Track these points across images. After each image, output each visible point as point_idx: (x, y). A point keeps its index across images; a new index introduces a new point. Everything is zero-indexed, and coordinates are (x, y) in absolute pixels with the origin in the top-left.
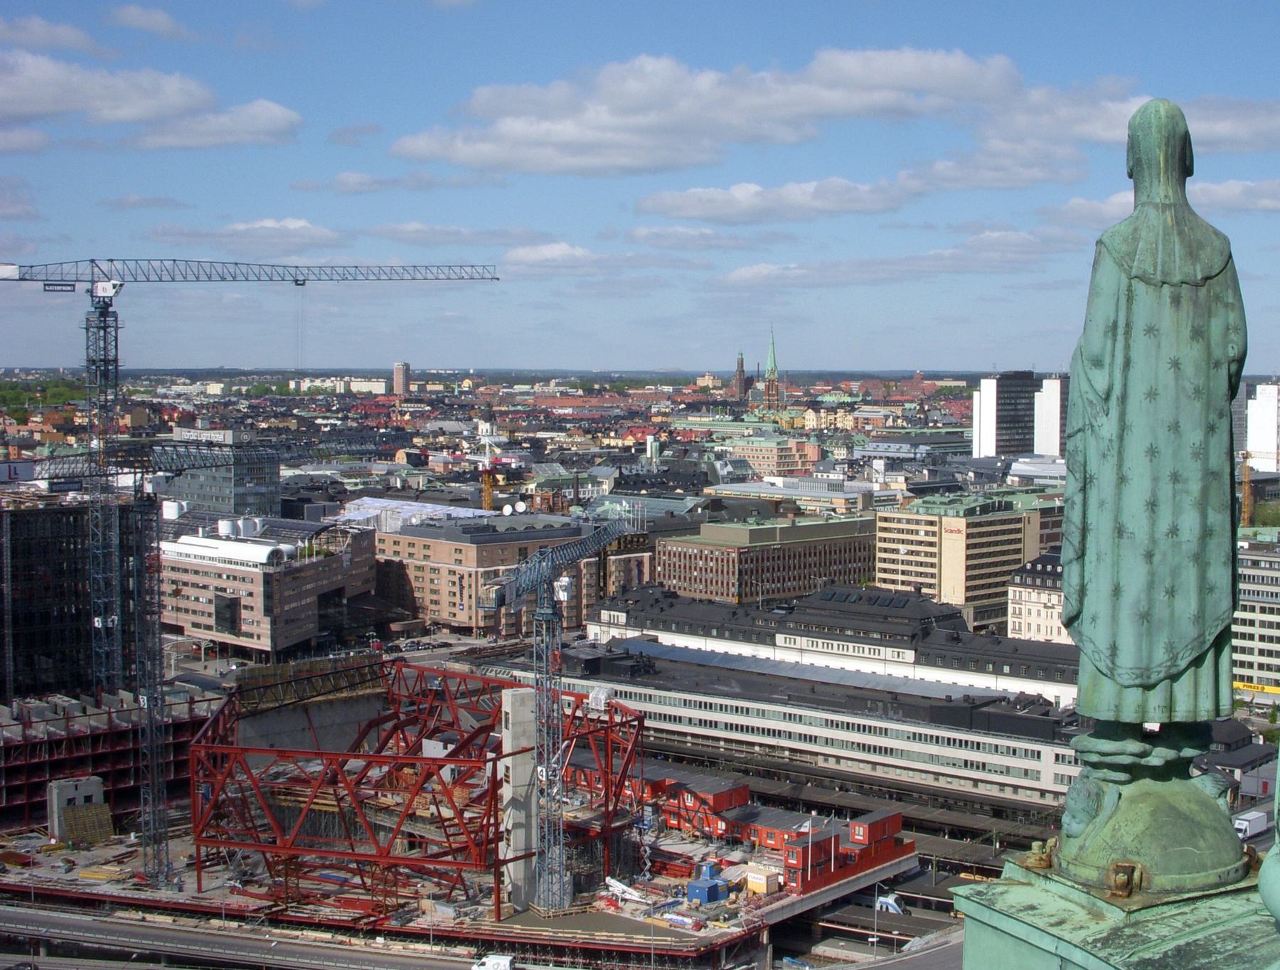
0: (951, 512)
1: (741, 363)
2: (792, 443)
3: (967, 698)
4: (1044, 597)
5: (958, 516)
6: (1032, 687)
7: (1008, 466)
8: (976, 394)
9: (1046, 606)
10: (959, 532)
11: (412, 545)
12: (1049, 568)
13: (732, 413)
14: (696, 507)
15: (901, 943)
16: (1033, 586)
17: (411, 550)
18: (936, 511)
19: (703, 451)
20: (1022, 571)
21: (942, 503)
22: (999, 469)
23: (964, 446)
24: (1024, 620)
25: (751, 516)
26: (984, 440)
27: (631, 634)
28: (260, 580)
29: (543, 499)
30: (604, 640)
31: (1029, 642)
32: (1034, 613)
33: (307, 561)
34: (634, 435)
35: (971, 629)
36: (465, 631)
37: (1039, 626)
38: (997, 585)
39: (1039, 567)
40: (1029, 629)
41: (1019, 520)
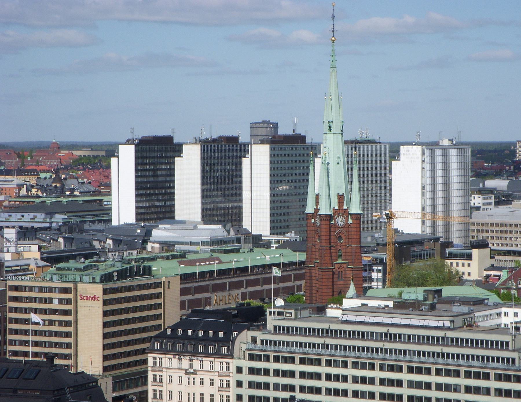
0: (86, 279)
4: (186, 363)
5: (94, 282)
7: (148, 233)
8: (114, 160)
9: (187, 372)
10: (95, 298)
12: (190, 332)
16: (174, 352)
20: (162, 336)
22: (138, 236)
24: (166, 387)
32: (175, 379)
37: (180, 393)
38: (136, 353)
39: (180, 332)
41: (158, 285)
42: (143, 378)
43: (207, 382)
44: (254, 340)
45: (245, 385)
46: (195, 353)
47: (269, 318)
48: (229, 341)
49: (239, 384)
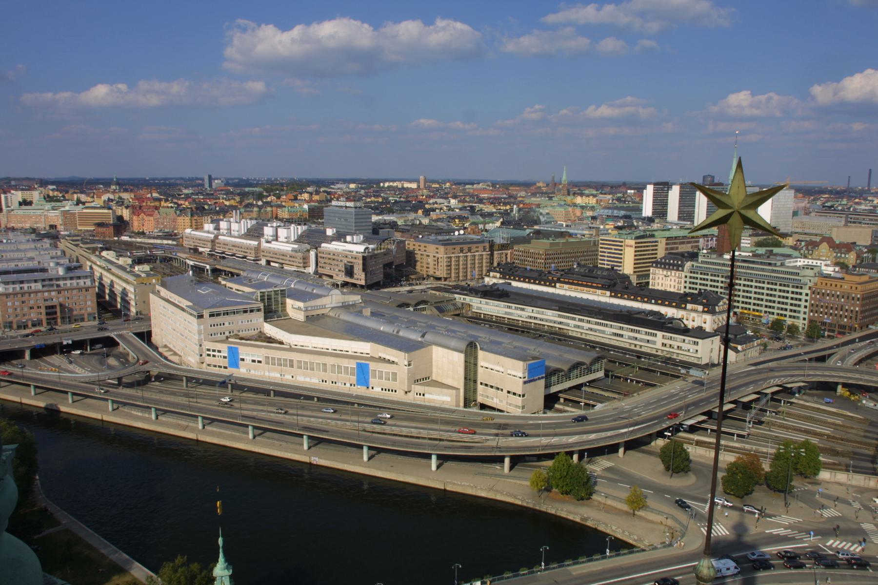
1: (553, 178)
2: (570, 209)
3: (628, 311)
4: (665, 273)
5: (632, 239)
6: (656, 308)
8: (645, 191)
9: (665, 276)
10: (631, 246)
11: (420, 246)
13: (548, 197)
14: (530, 233)
15: (594, 406)
16: (661, 268)
17: (420, 248)
18: (623, 237)
19: (535, 212)
20: (657, 263)
21: (626, 234)
23: (640, 210)
24: (656, 281)
25: (551, 237)
26: (647, 210)
27: (501, 281)
28: (361, 258)
29: (471, 229)
30: (491, 283)
31: (658, 290)
32: (661, 278)
33: (379, 251)
34: (510, 205)
35: (635, 285)
36: (439, 279)
39: (663, 260)
40: (658, 285)
41: (656, 242)
42: (648, 275)
43: (673, 280)
44: (693, 266)
45: (688, 282)
46: (669, 269)
47: (700, 257)
48: (682, 266)
49: (686, 282)
